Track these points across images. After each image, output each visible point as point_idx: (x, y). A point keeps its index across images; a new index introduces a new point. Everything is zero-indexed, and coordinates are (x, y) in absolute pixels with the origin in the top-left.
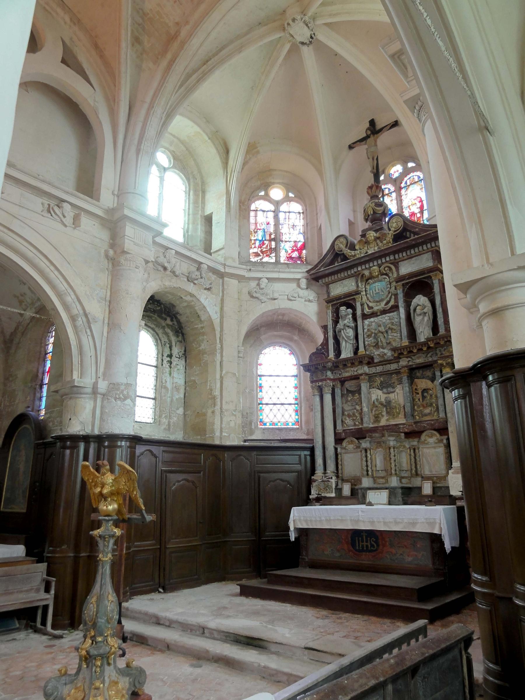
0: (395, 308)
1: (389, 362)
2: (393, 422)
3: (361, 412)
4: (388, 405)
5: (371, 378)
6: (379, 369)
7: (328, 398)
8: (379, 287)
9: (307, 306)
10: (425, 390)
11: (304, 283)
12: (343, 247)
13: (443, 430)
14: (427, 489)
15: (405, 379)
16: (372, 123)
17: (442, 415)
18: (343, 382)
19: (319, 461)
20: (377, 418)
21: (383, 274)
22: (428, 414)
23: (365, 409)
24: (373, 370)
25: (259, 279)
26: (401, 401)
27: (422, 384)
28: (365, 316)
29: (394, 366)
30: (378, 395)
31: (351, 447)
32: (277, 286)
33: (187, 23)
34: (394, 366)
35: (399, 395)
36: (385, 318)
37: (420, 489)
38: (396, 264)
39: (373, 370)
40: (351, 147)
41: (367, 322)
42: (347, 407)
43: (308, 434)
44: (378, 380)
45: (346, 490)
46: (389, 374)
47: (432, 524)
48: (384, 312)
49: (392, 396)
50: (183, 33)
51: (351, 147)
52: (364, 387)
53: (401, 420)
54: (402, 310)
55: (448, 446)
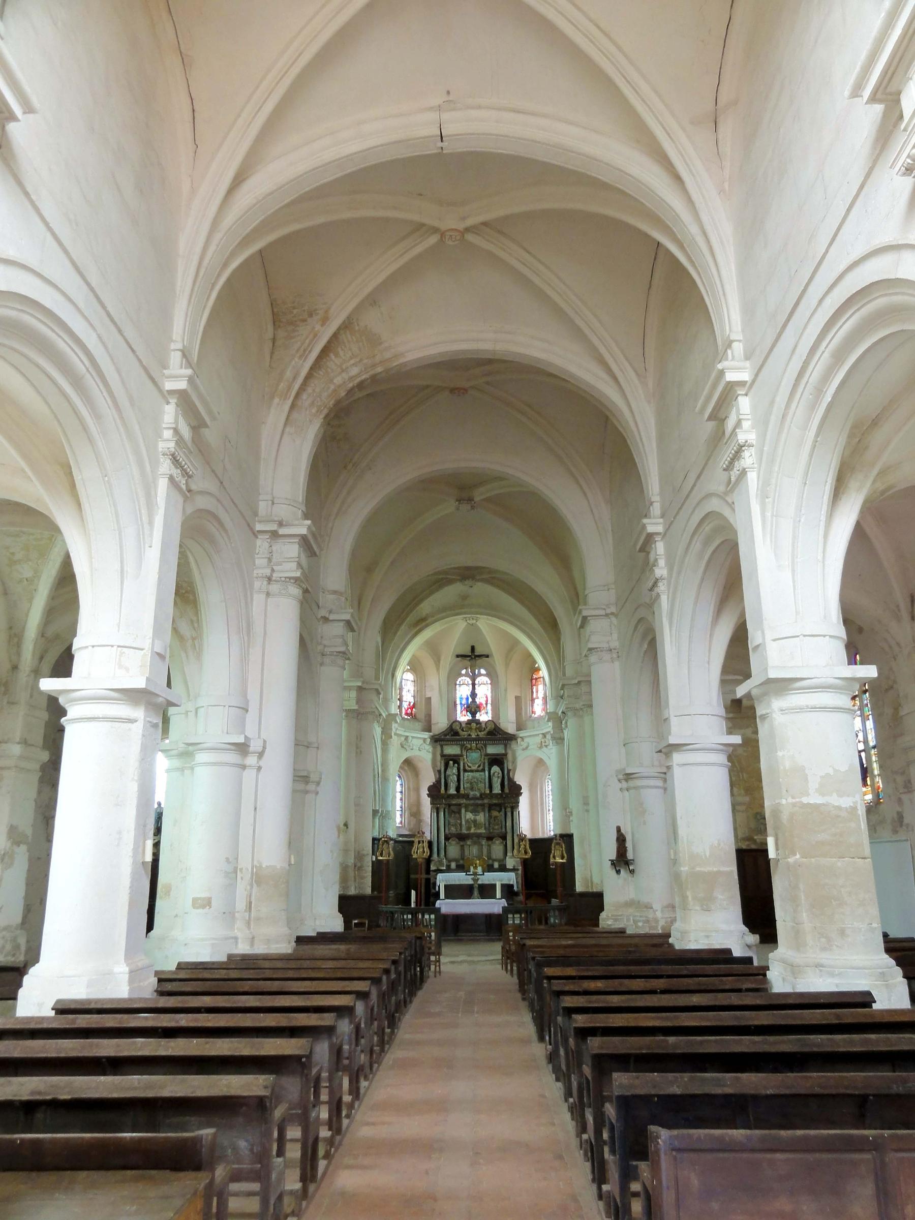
0: (483, 770)
1: (478, 799)
2: (479, 831)
3: (461, 824)
4: (475, 821)
5: (466, 807)
6: (472, 802)
7: (442, 814)
8: (475, 755)
9: (423, 753)
10: (496, 817)
11: (429, 740)
12: (458, 728)
13: (504, 838)
14: (496, 865)
15: (487, 810)
16: (473, 648)
17: (504, 830)
18: (450, 805)
19: (435, 849)
20: (469, 828)
21: (477, 748)
22: (497, 829)
23: (463, 823)
24: (468, 802)
25: (407, 738)
26: (483, 820)
27: (495, 813)
28: (465, 771)
29: (480, 802)
30: (470, 816)
31: (454, 842)
32: (415, 741)
33: (433, 616)
34: (480, 802)
35: (481, 817)
36: (477, 774)
37: (492, 865)
38: (485, 746)
39: (468, 802)
40: (458, 656)
41: (466, 774)
42: (452, 821)
43: (409, 830)
44: (471, 808)
45: (453, 865)
46: (477, 805)
47: (510, 880)
48: (477, 771)
49: (478, 817)
50: (430, 620)
51: (458, 656)
52: (463, 811)
53: (482, 831)
54: (487, 773)
55: (506, 846)
